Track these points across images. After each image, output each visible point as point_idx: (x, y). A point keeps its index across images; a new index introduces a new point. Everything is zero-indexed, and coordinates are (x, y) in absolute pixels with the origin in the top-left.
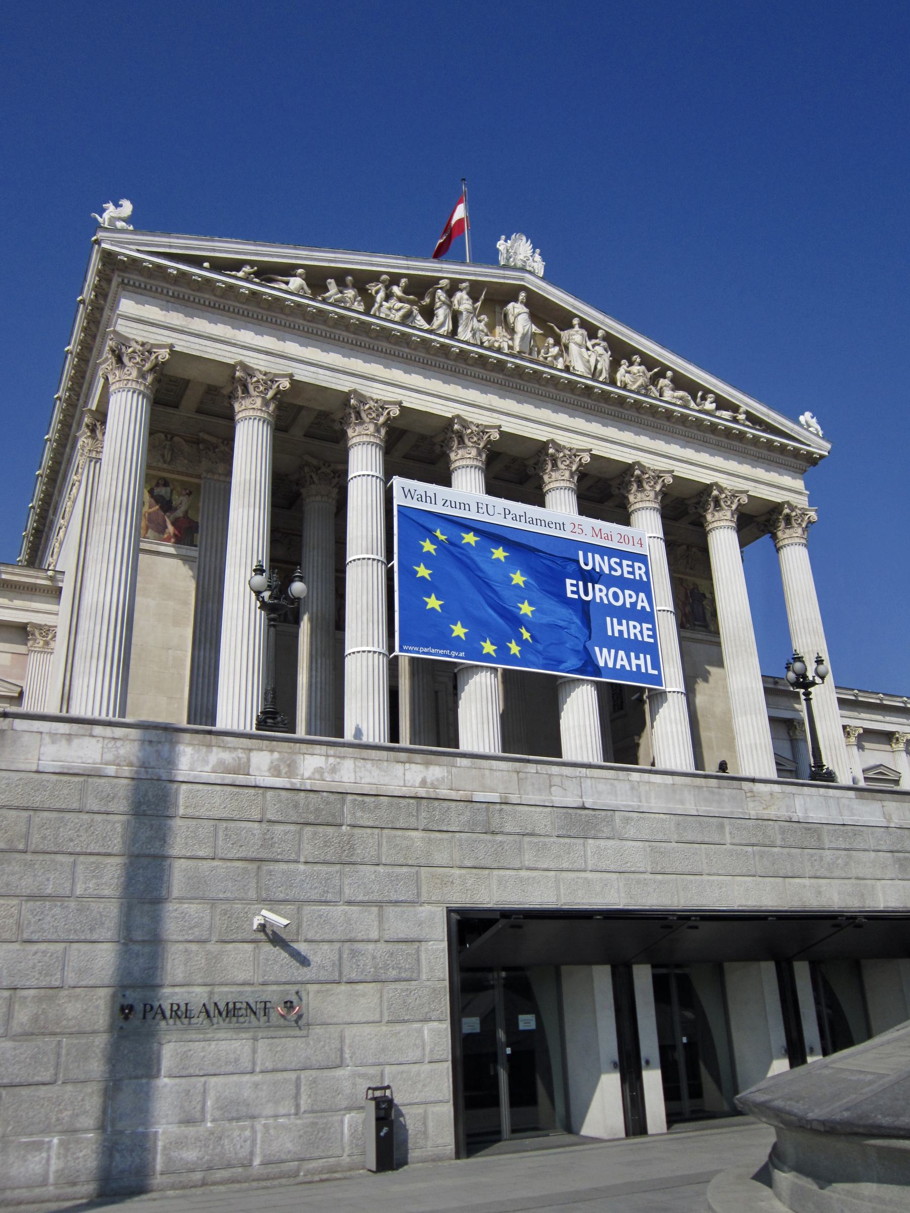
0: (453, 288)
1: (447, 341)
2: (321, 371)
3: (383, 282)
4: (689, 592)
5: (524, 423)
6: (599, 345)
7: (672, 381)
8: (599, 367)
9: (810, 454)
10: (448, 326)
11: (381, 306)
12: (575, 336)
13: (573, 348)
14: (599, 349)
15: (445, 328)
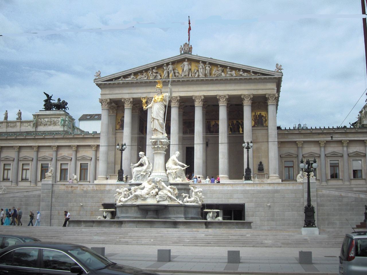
0: (168, 64)
1: (165, 80)
2: (139, 94)
3: (150, 70)
4: (257, 116)
5: (187, 92)
6: (207, 66)
7: (230, 69)
8: (206, 73)
9: (275, 78)
10: (166, 75)
11: (151, 75)
12: (201, 65)
13: (199, 70)
14: (207, 68)
15: (166, 76)
